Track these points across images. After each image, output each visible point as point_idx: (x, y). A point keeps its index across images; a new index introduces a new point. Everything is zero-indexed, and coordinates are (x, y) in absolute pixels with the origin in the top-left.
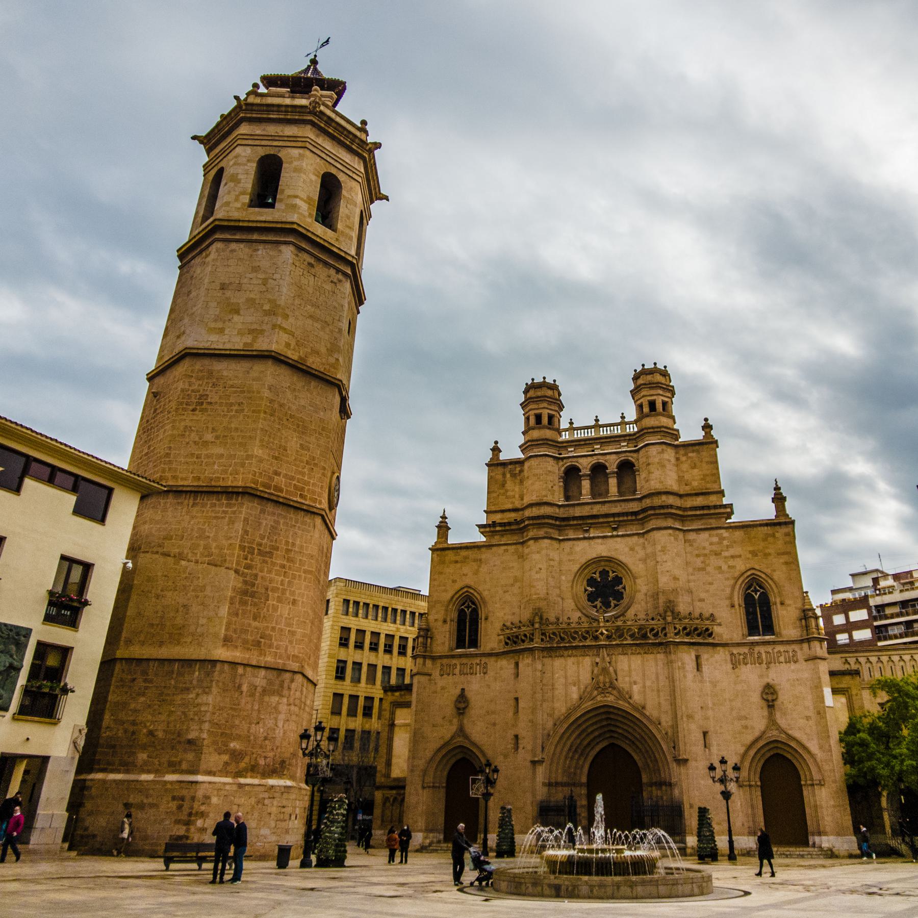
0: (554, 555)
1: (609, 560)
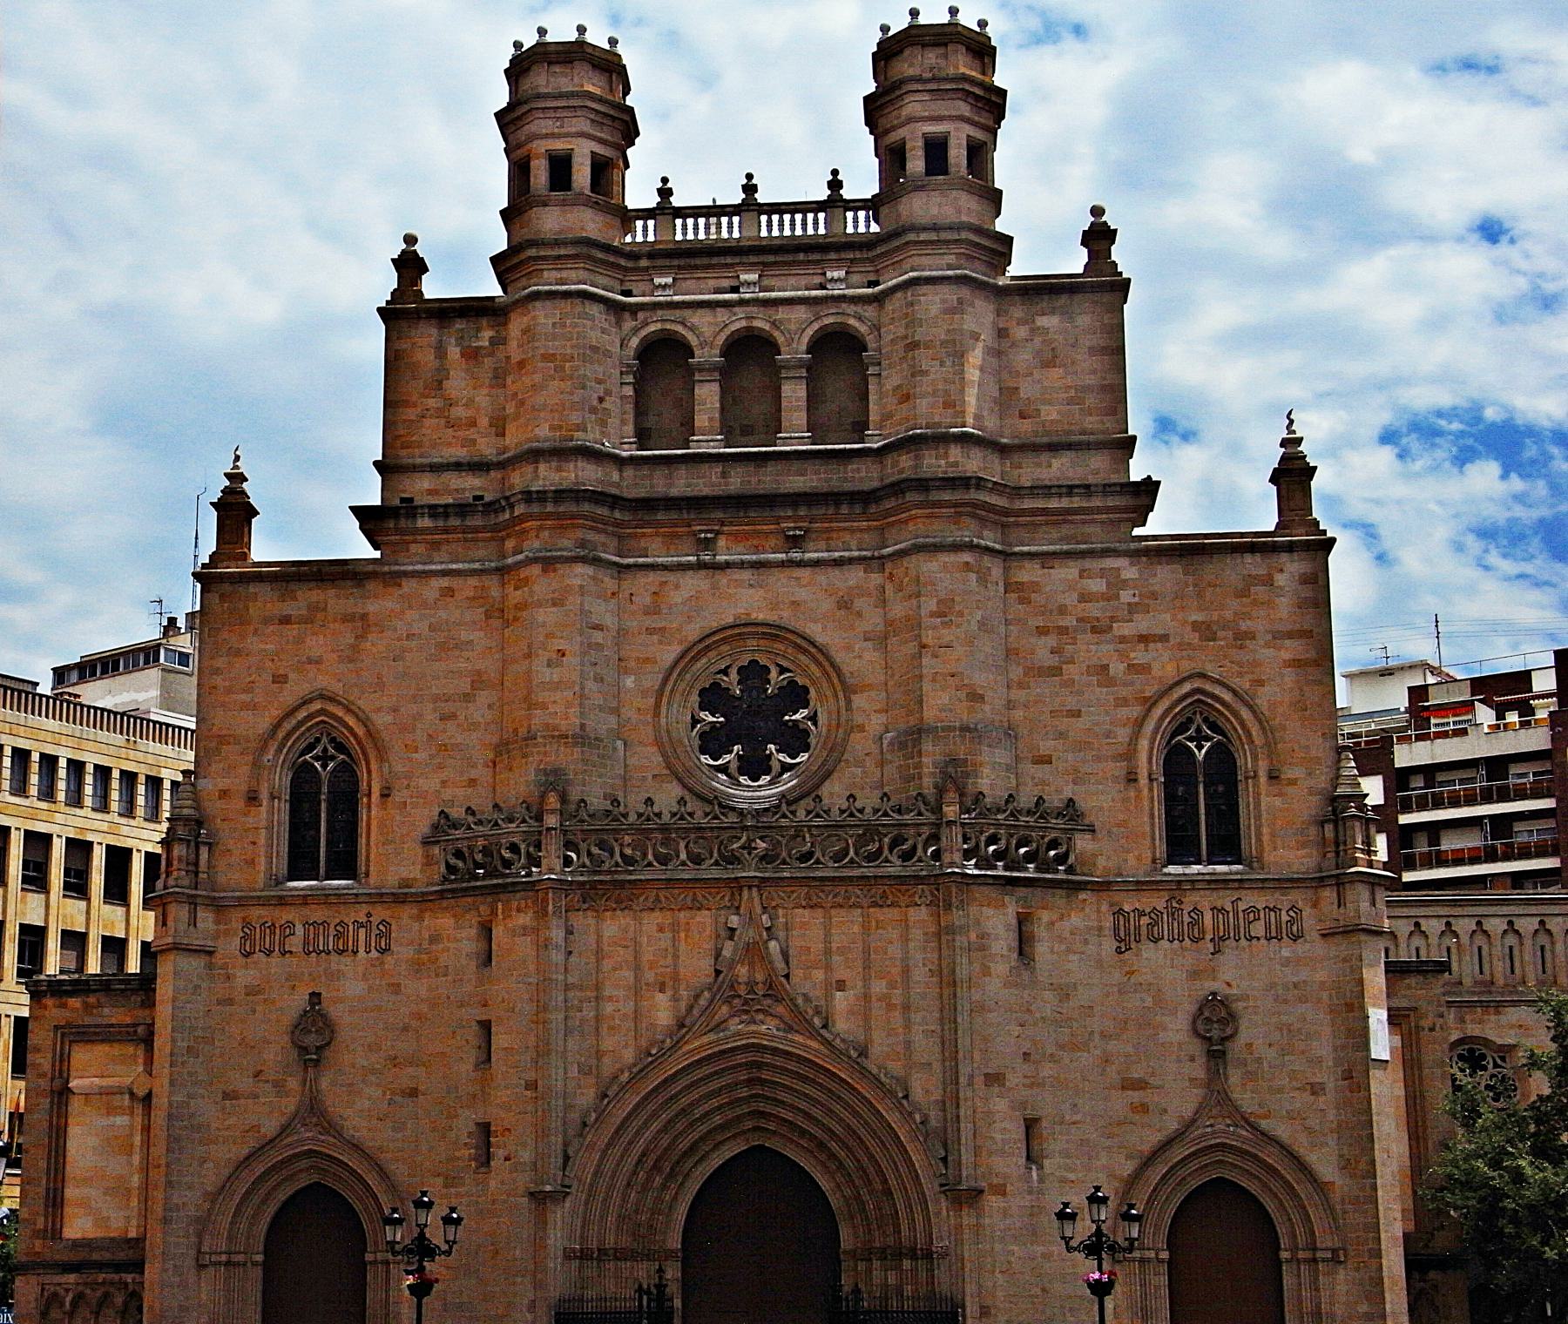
0: (603, 612)
1: (774, 632)
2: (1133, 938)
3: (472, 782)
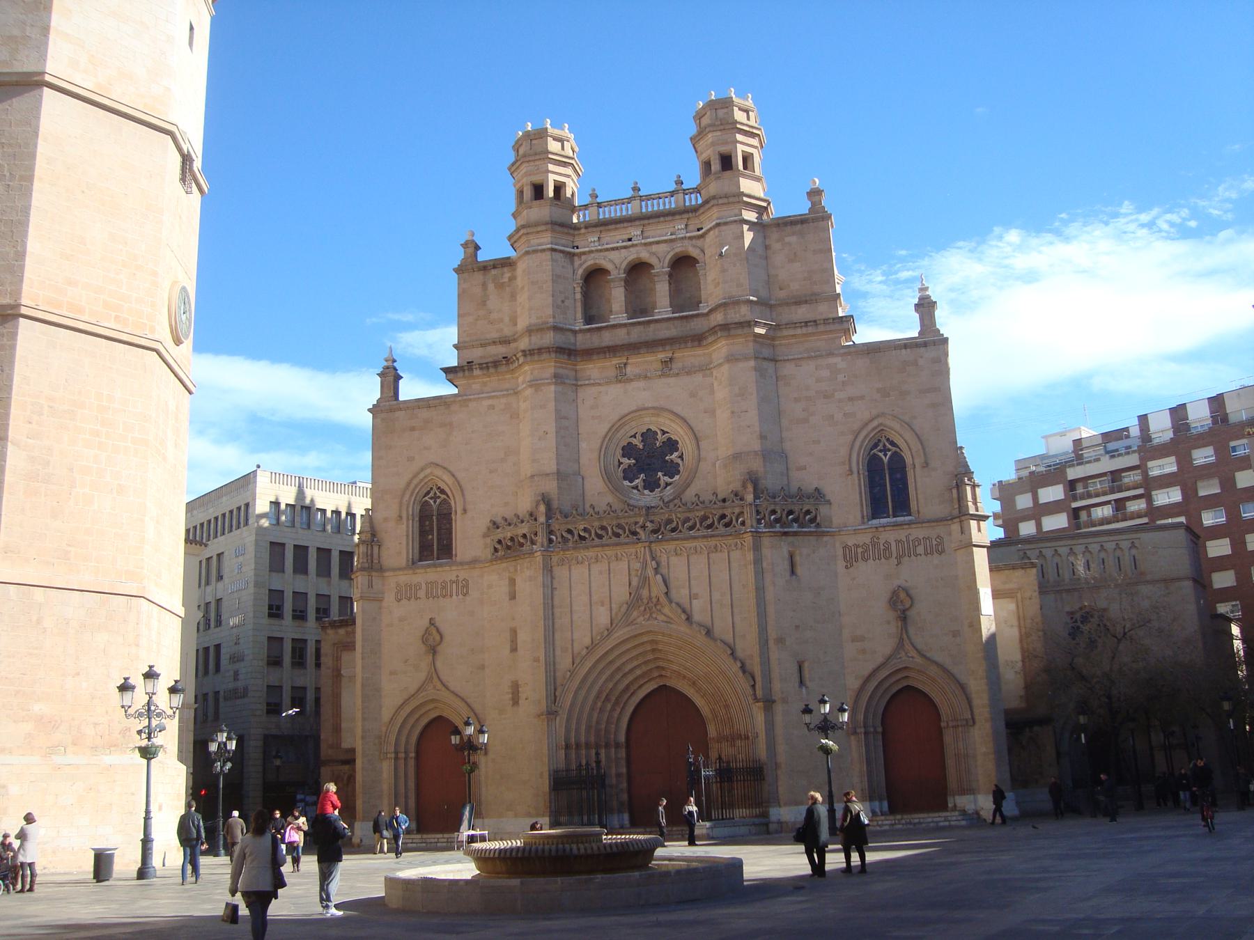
2: (854, 560)
3: (506, 504)
